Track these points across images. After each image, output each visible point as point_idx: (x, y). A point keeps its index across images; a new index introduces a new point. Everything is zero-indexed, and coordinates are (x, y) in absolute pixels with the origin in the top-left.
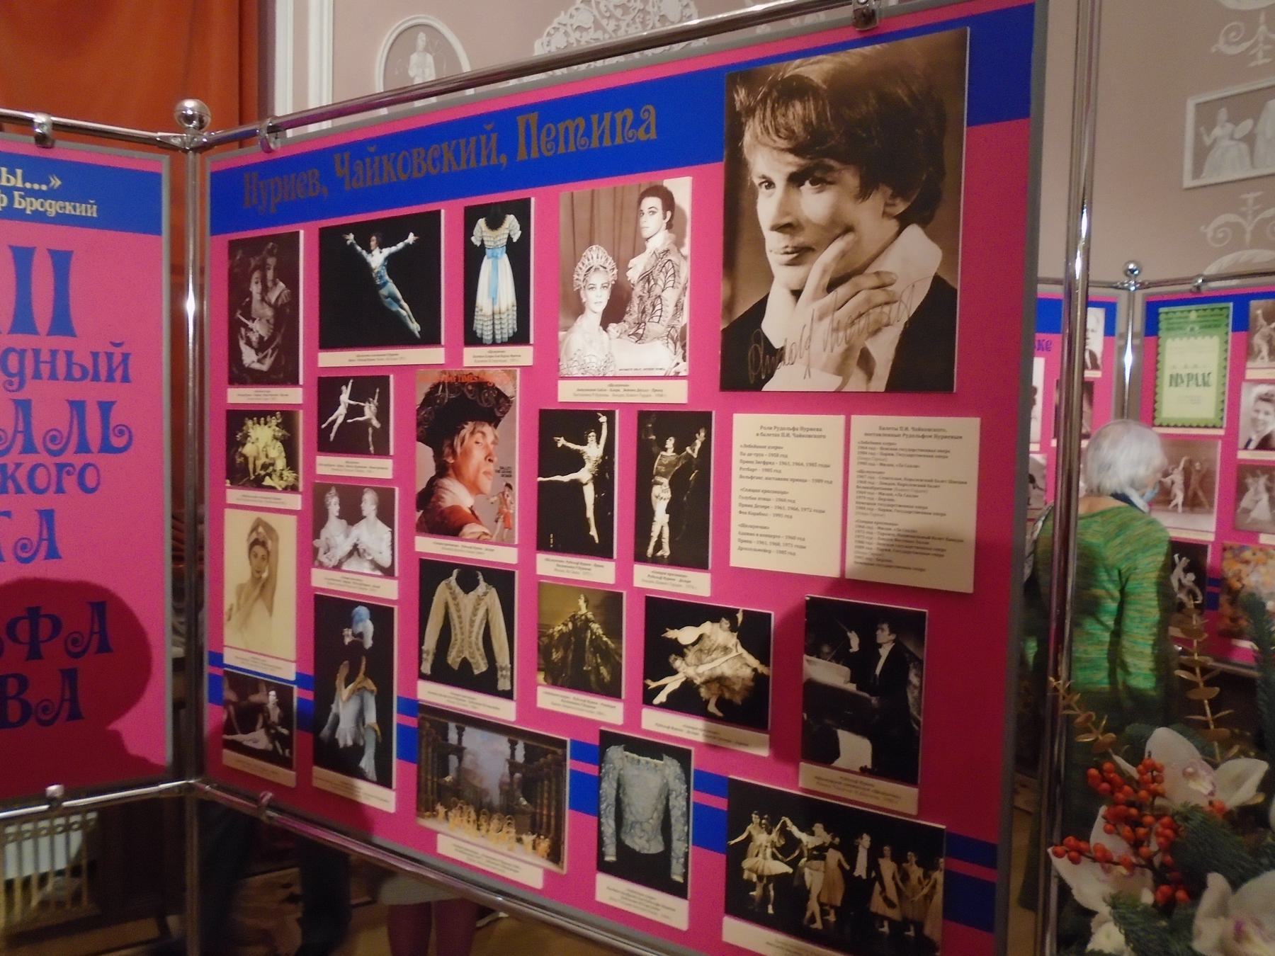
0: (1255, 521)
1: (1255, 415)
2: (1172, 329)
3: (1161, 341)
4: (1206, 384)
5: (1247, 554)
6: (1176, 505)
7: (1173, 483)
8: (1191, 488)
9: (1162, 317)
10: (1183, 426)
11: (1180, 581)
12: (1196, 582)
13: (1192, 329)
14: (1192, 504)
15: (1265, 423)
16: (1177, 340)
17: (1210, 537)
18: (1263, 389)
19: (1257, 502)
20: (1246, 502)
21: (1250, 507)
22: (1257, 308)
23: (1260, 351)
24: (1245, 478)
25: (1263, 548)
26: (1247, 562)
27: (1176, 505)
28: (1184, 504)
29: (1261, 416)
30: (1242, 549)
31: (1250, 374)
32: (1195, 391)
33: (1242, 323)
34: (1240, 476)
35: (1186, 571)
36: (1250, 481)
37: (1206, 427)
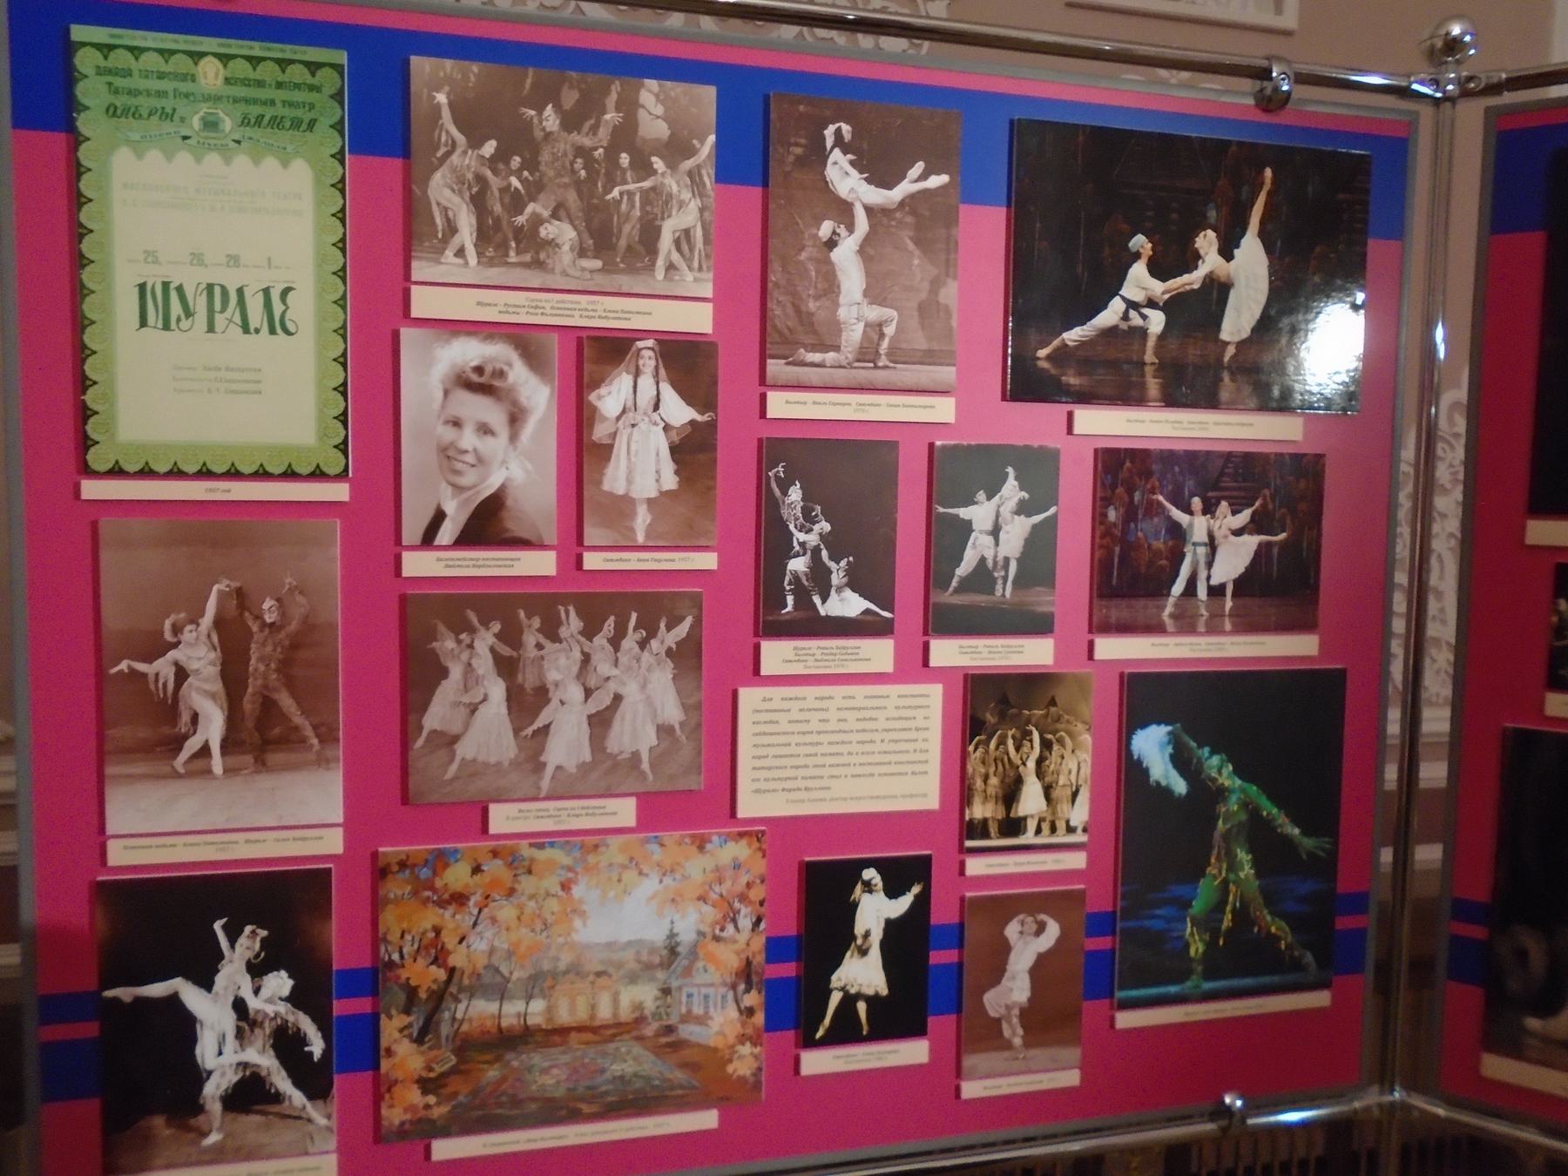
0: (473, 769)
1: (448, 434)
2: (126, 112)
3: (85, 154)
4: (277, 325)
5: (457, 876)
6: (205, 751)
7: (181, 674)
8: (253, 686)
9: (85, 61)
10: (205, 474)
11: (239, 1006)
12: (296, 999)
13: (211, 124)
14: (259, 738)
15: (480, 460)
16: (154, 155)
17: (333, 843)
18: (468, 352)
19: (473, 709)
20: (437, 716)
21: (455, 728)
22: (435, 83)
23: (452, 229)
24: (432, 635)
25: (506, 851)
26: (459, 899)
27: (205, 751)
28: (227, 746)
29: (469, 439)
30: (440, 861)
31: (424, 303)
32: (231, 346)
33: (380, 126)
34: (414, 636)
35: (257, 970)
36: (447, 644)
37: (290, 475)
